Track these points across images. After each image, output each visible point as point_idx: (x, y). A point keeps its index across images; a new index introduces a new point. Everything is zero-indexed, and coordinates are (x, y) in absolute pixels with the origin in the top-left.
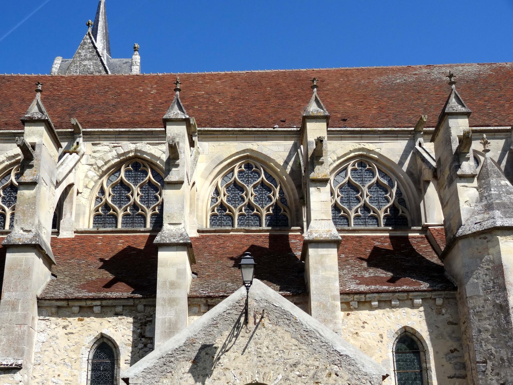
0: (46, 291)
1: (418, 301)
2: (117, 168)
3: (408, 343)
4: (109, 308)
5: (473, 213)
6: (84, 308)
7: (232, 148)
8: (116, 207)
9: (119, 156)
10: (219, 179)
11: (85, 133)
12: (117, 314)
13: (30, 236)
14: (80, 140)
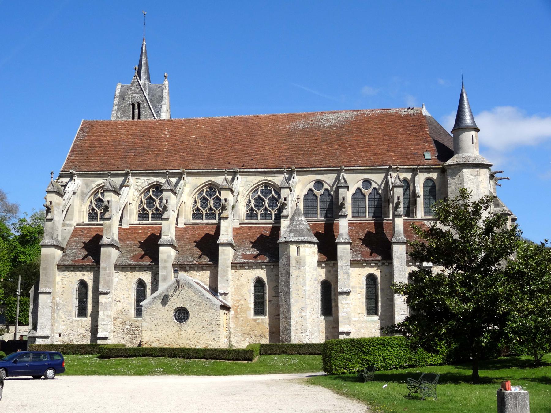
0: (117, 261)
1: (264, 267)
2: (148, 189)
3: (259, 282)
4: (141, 268)
5: (286, 232)
6: (132, 268)
7: (202, 180)
8: (148, 210)
9: (148, 184)
10: (196, 196)
11: (132, 173)
12: (145, 271)
13: (109, 241)
14: (130, 177)
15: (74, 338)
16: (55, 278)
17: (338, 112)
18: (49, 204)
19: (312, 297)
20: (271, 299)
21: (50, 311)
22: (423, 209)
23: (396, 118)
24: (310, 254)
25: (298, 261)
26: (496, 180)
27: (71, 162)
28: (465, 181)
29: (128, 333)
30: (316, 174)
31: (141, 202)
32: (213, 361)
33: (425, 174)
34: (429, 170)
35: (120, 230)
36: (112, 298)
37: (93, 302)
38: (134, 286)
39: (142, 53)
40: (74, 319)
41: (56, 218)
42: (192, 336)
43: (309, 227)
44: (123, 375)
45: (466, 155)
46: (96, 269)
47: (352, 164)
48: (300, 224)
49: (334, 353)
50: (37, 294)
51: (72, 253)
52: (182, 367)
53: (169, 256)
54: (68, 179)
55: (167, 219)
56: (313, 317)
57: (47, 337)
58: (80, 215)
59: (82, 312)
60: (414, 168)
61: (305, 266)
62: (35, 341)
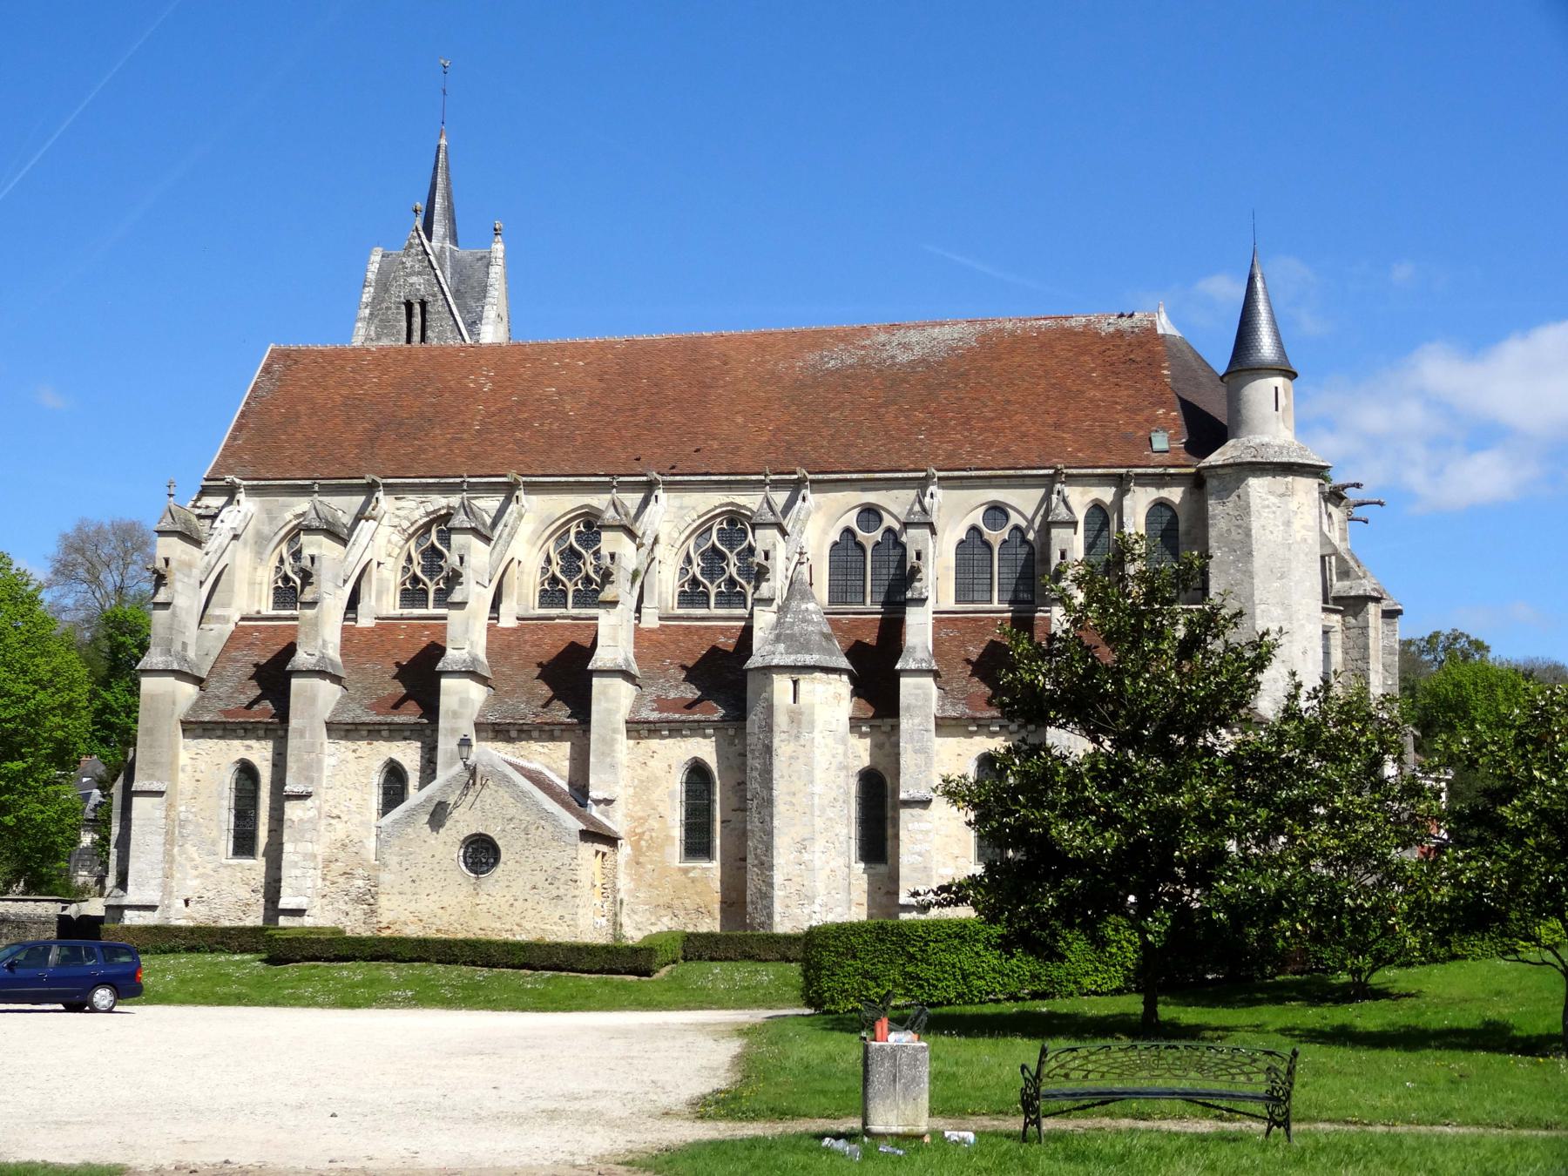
0: (335, 712)
2: (427, 528)
3: (697, 773)
4: (396, 732)
5: (765, 641)
6: (373, 732)
8: (426, 580)
9: (428, 514)
10: (551, 544)
11: (385, 485)
12: (405, 739)
13: (313, 660)
14: (380, 495)
15: (221, 912)
16: (176, 756)
17: (933, 326)
18: (160, 564)
19: (830, 813)
20: (725, 816)
21: (161, 839)
23: (1084, 342)
24: (830, 700)
25: (795, 718)
26: (1347, 506)
27: (233, 455)
28: (1253, 508)
29: (359, 900)
30: (863, 490)
31: (409, 559)
32: (549, 974)
33: (1150, 489)
34: (1160, 481)
35: (348, 635)
36: (319, 809)
37: (271, 817)
38: (376, 779)
39: (436, 168)
40: (224, 861)
41: (180, 601)
42: (505, 908)
43: (827, 629)
44: (308, 1006)
45: (1256, 439)
46: (280, 733)
47: (958, 463)
48: (804, 620)
49: (828, 959)
50: (128, 795)
51: (223, 690)
52: (464, 988)
53: (464, 702)
54: (224, 499)
55: (461, 605)
56: (833, 864)
57: (152, 908)
58: (251, 593)
59: (244, 843)
60: (1120, 475)
61: (816, 731)
62: (121, 916)
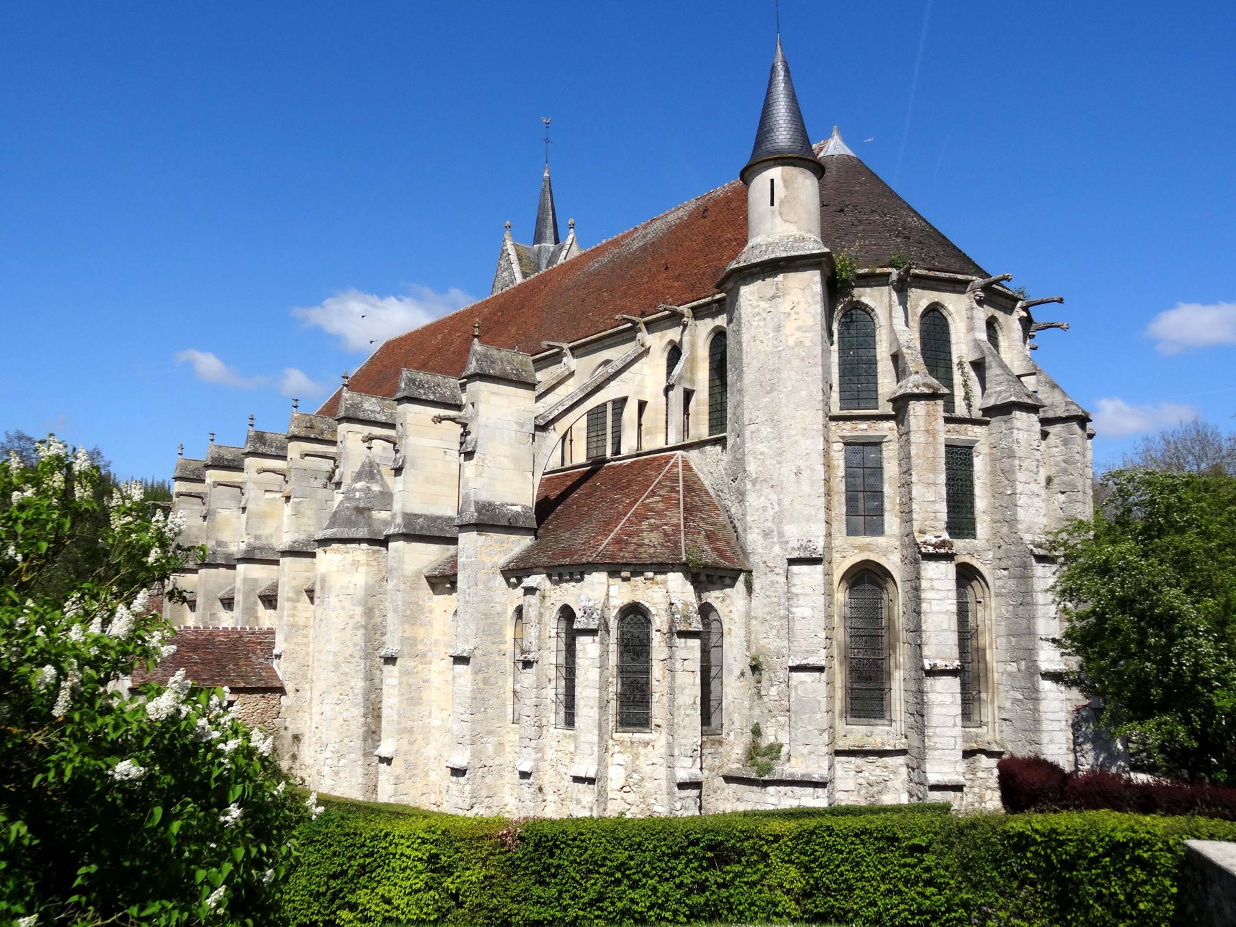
22: (707, 417)
26: (973, 290)
33: (708, 320)
